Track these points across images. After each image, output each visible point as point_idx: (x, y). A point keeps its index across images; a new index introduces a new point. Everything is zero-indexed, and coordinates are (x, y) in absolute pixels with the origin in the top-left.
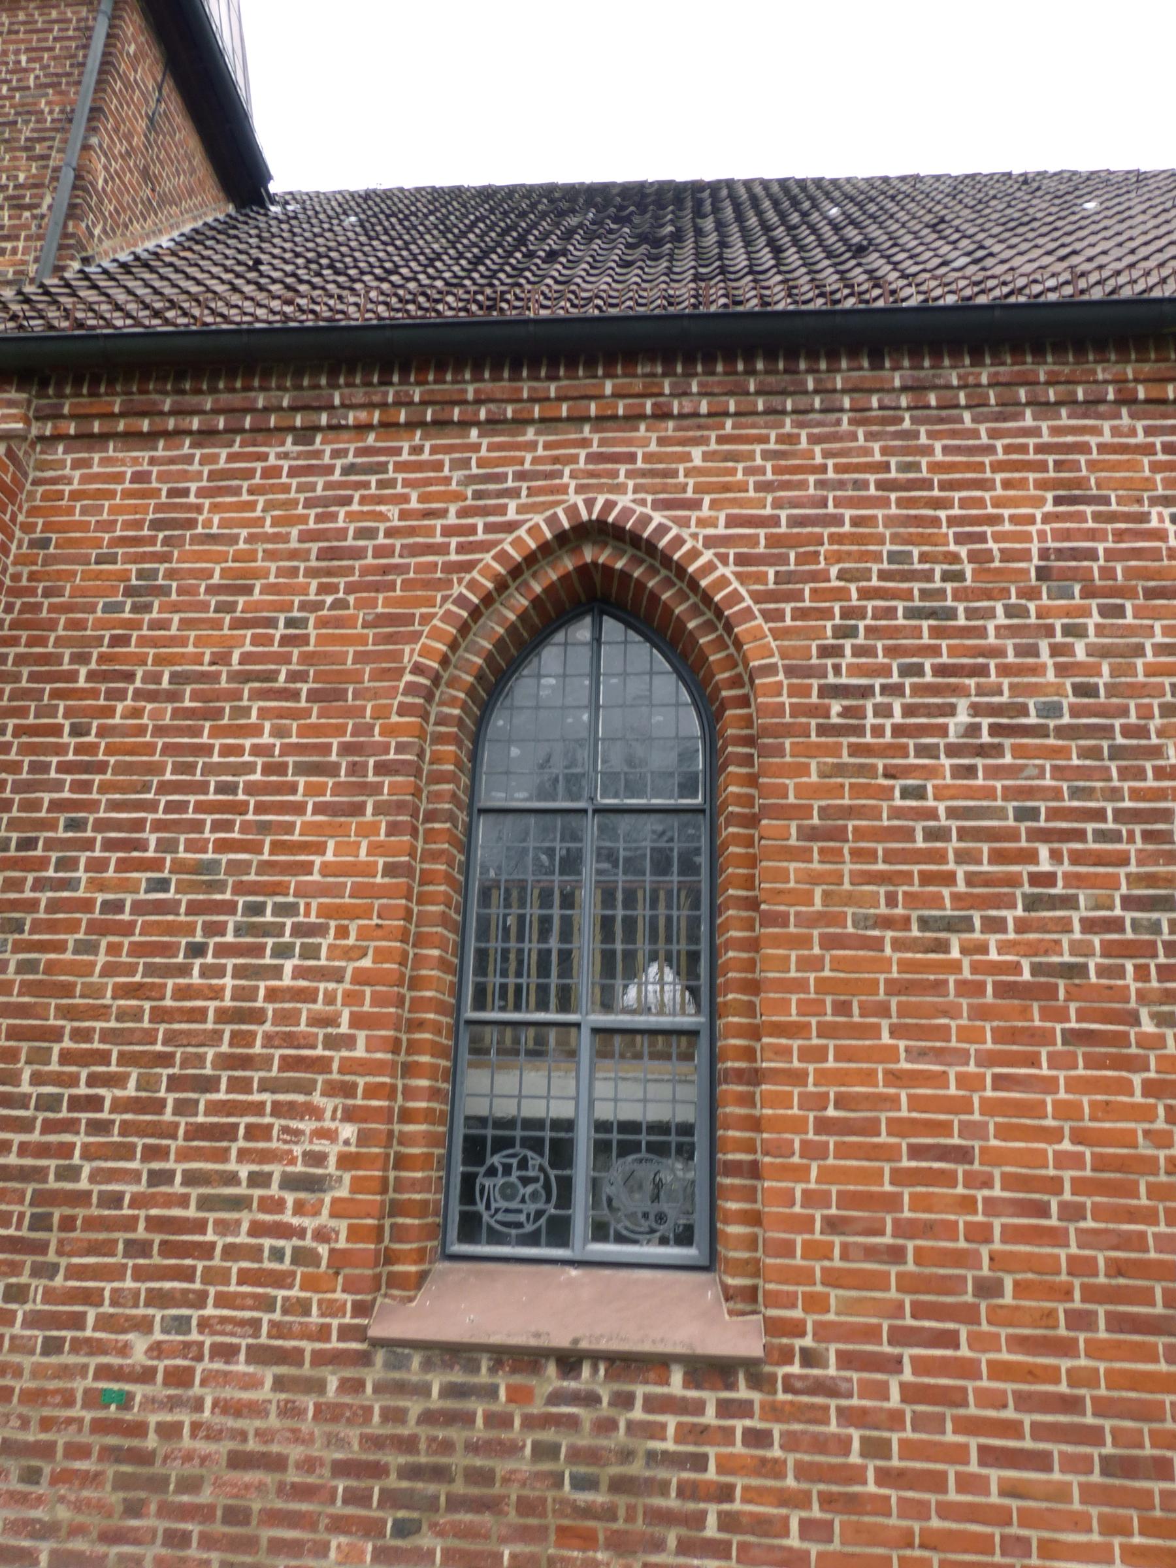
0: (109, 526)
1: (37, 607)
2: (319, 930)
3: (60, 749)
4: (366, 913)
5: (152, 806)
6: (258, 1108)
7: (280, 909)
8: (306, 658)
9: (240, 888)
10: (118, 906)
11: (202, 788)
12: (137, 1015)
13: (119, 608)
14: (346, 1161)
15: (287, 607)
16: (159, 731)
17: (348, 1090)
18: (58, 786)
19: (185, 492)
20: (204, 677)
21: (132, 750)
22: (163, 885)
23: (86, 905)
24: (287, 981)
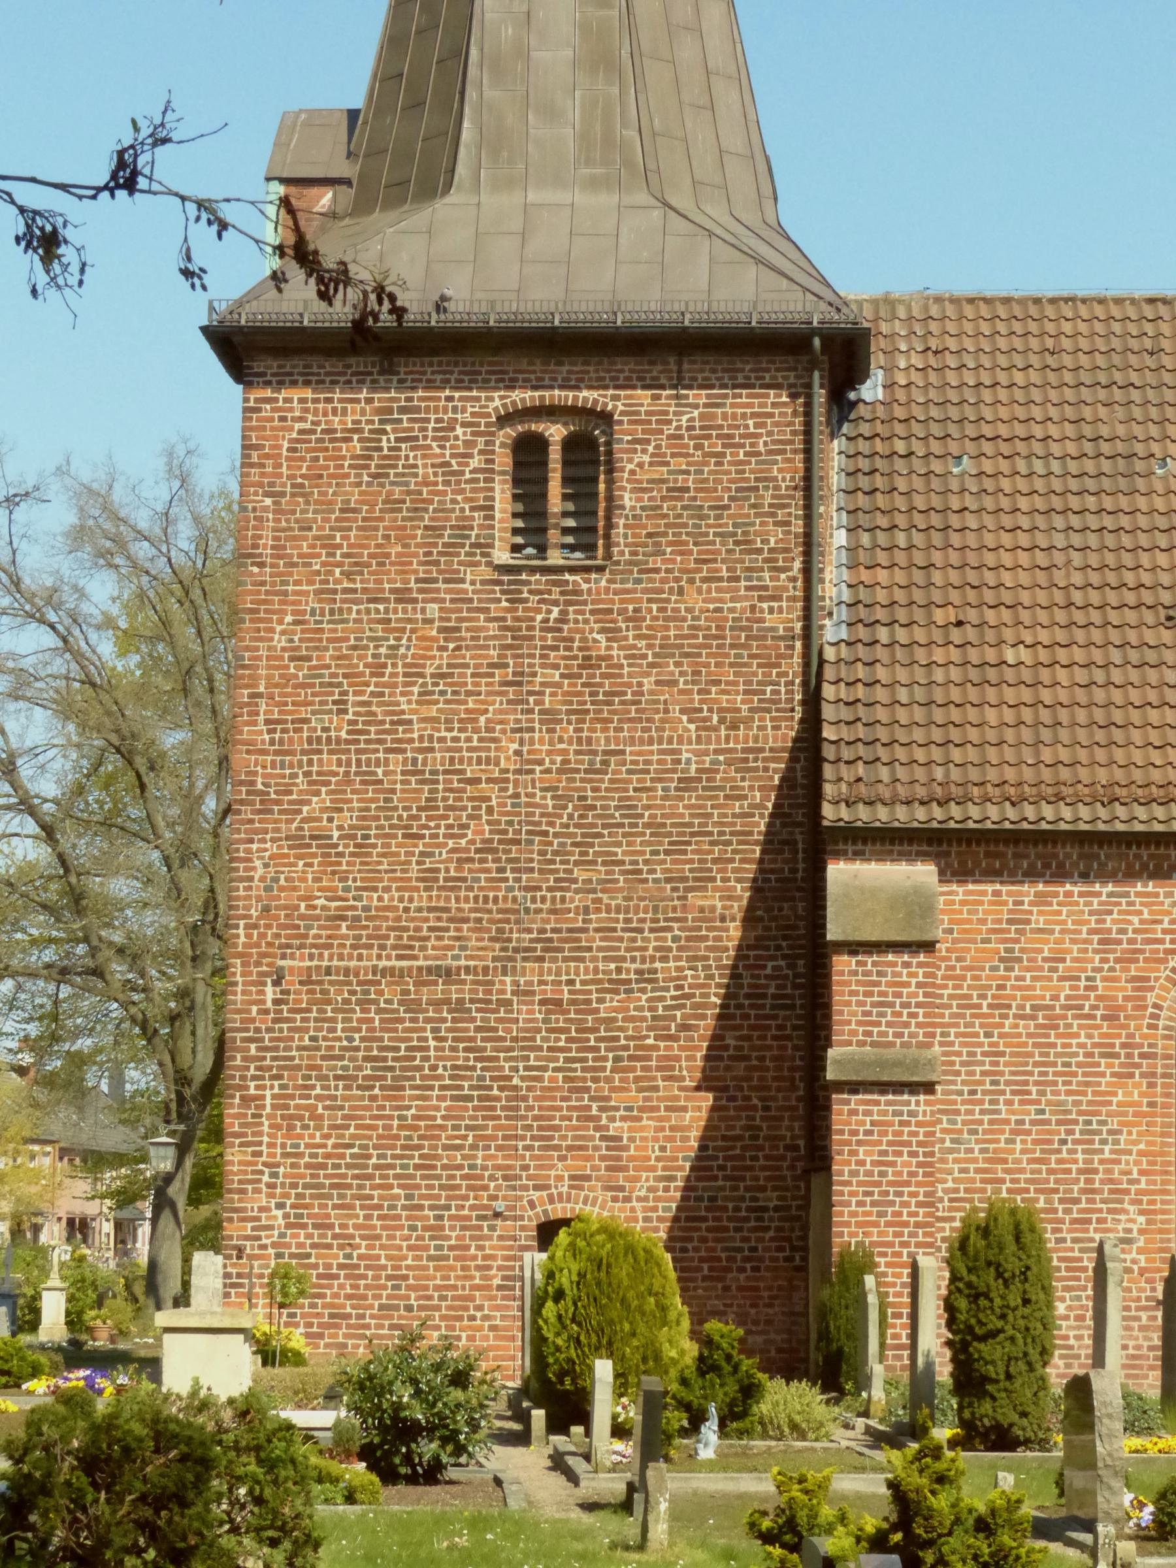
0: (983, 921)
1: (953, 968)
2: (1119, 1132)
3: (981, 1045)
4: (1139, 1124)
5: (1031, 1074)
6: (1100, 1211)
7: (1100, 1123)
8: (1098, 998)
9: (1080, 1113)
10: (1022, 1122)
11: (1055, 1064)
12: (1039, 1172)
13: (996, 968)
14: (1141, 1232)
15: (1085, 970)
16: (1029, 1035)
17: (1140, 1202)
18: (983, 1063)
19: (1022, 903)
20: (1047, 1007)
21: (1019, 1045)
22: (1042, 1112)
23: (1007, 1122)
24: (1107, 1155)
